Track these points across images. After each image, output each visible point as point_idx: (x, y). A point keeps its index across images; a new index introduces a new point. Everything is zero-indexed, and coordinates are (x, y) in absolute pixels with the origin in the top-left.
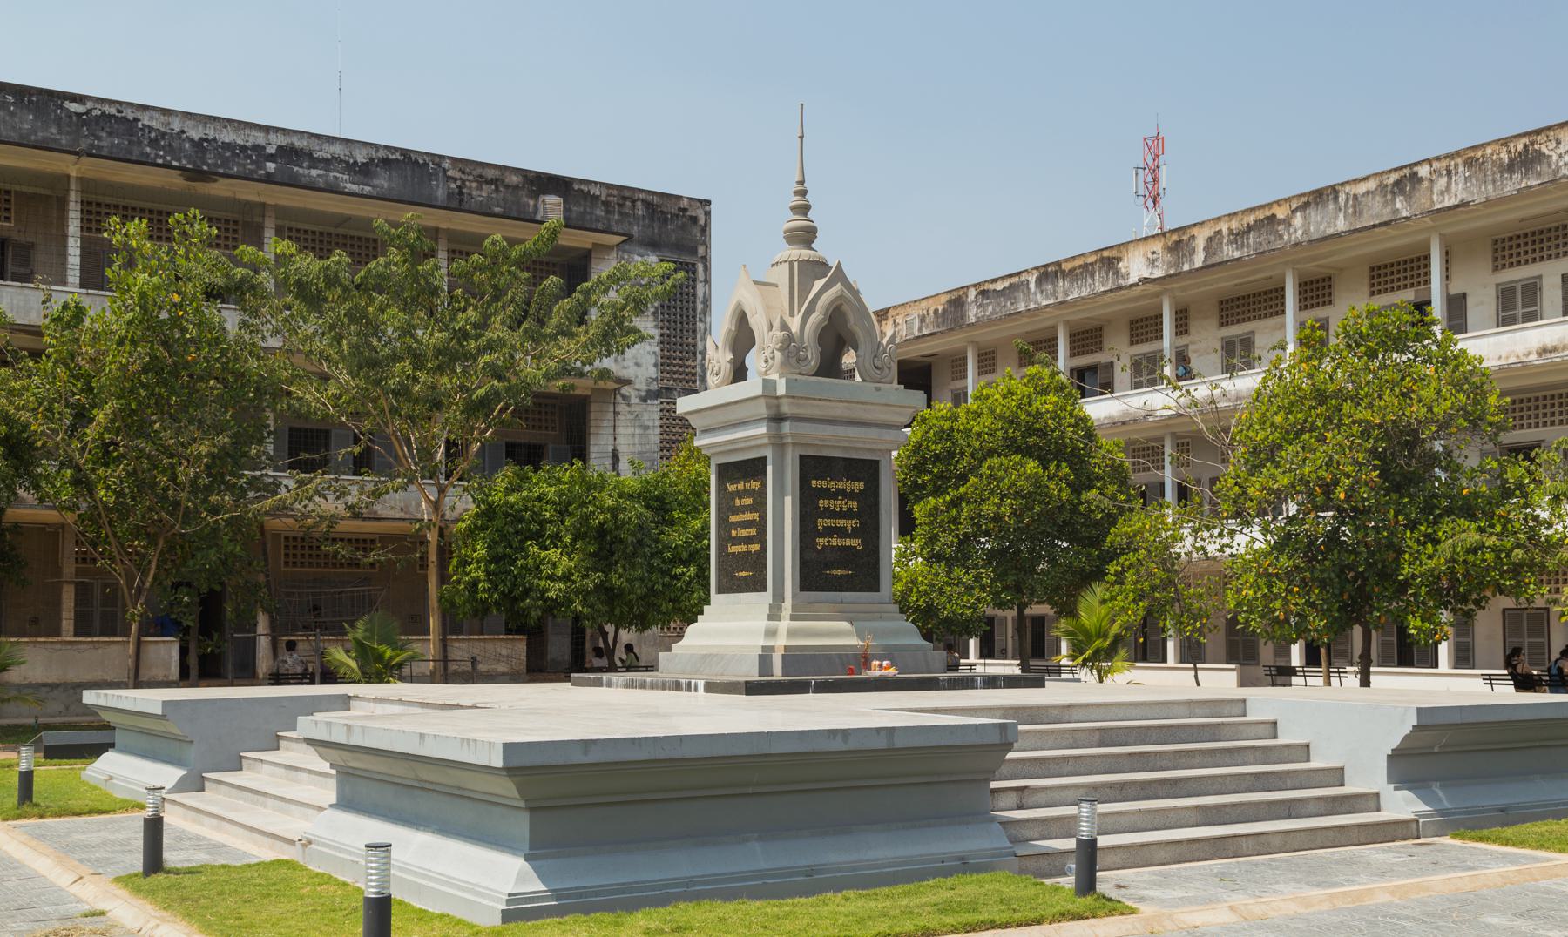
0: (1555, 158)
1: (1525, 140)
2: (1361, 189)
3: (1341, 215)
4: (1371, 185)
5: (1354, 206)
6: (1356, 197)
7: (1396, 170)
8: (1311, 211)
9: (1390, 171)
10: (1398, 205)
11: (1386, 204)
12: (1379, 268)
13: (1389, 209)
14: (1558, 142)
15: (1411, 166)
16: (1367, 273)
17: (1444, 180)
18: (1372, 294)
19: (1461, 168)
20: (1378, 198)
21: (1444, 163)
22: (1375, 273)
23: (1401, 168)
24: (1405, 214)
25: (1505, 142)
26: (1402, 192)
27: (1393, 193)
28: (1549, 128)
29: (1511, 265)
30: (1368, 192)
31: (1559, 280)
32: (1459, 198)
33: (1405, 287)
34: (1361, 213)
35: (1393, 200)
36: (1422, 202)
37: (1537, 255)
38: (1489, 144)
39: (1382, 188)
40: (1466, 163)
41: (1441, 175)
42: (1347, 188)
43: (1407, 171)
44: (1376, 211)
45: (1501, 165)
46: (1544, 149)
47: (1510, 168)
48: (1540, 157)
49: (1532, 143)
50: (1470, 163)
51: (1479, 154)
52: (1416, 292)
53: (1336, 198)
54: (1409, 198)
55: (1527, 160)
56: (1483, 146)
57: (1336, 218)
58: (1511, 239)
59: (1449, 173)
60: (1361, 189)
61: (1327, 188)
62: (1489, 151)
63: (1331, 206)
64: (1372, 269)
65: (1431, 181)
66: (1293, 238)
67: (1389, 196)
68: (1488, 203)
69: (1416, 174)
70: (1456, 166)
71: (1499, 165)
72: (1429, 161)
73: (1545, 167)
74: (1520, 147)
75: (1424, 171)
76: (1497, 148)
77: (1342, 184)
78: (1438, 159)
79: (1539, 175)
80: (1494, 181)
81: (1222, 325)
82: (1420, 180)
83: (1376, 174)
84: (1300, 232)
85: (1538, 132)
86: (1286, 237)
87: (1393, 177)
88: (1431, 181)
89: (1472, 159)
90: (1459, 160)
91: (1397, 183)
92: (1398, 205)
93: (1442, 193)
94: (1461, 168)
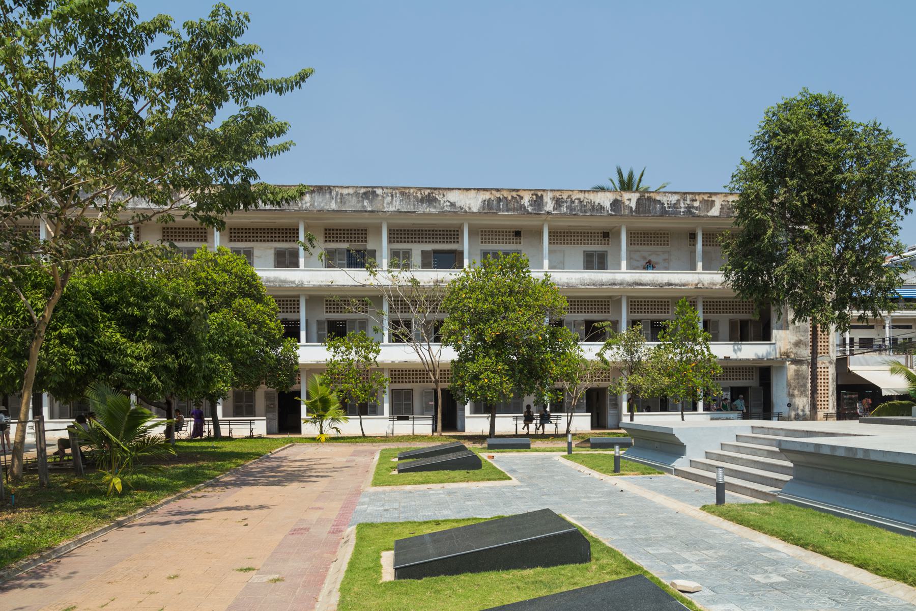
0: (442, 202)
1: (429, 191)
2: (345, 191)
3: (334, 202)
4: (351, 191)
5: (341, 199)
6: (342, 194)
7: (364, 187)
8: (316, 195)
9: (361, 187)
10: (365, 204)
11: (358, 202)
12: (330, 230)
13: (360, 205)
14: (444, 196)
15: (373, 187)
16: (323, 232)
17: (389, 199)
18: (326, 241)
19: (398, 195)
20: (354, 198)
21: (390, 191)
22: (328, 232)
23: (367, 187)
24: (369, 209)
25: (420, 189)
26: (367, 198)
27: (362, 197)
28: (440, 189)
29: (398, 242)
30: (349, 194)
31: (420, 253)
32: (397, 208)
33: (344, 241)
34: (345, 203)
35: (363, 201)
36: (377, 205)
37: (410, 240)
38: (412, 188)
39: (357, 194)
40: (400, 193)
41: (388, 195)
42: (337, 189)
43: (370, 189)
44: (353, 205)
45: (418, 198)
46: (437, 197)
47: (423, 200)
48: (435, 200)
49: (432, 193)
50: (402, 194)
51: (407, 191)
52: (350, 245)
53: (330, 193)
54: (371, 202)
55: (430, 200)
56: (409, 188)
57: (331, 202)
58: (397, 230)
59: (392, 196)
60: (345, 191)
61: (325, 186)
62: (412, 191)
63: (328, 196)
64: (326, 230)
65: (383, 197)
66: (304, 206)
67: (360, 199)
68: (424, 214)
69: (375, 192)
70: (396, 194)
71: (416, 198)
72: (382, 188)
73: (438, 205)
74: (427, 193)
75: (379, 191)
76: (416, 191)
77: (334, 187)
78: (387, 188)
79: (435, 207)
80: (414, 205)
81: (231, 241)
82: (377, 195)
83: (354, 187)
84: (308, 204)
85: (435, 189)
86: (300, 205)
87: (363, 191)
88: (383, 197)
89: (404, 192)
90: (397, 191)
91: (364, 193)
92: (365, 204)
93: (388, 204)
94: (398, 195)
